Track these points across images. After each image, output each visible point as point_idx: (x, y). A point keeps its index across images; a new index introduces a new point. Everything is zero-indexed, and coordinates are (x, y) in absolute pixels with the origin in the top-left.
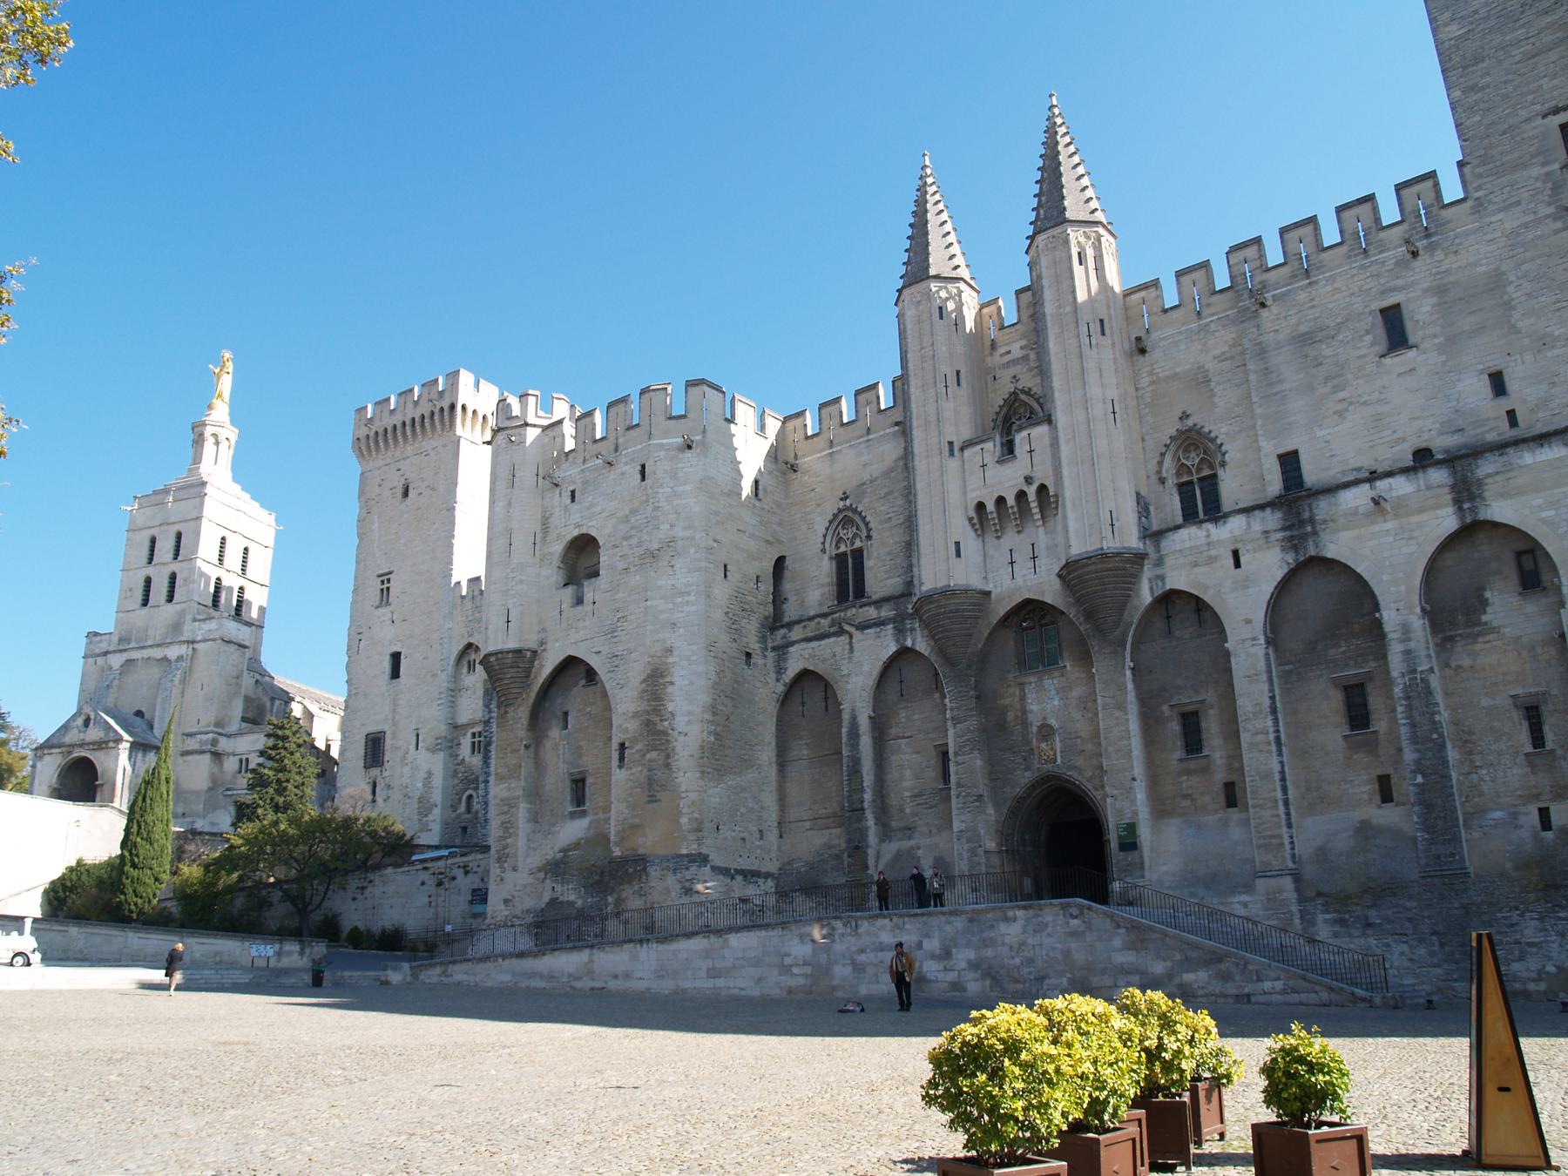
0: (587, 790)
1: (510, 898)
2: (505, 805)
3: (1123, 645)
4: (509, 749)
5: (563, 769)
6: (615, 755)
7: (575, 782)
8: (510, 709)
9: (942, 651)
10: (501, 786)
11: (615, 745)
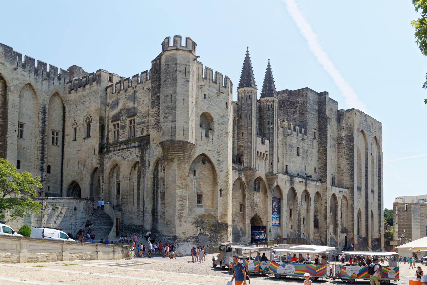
0: (203, 199)
1: (185, 232)
2: (181, 198)
3: (272, 192)
4: (182, 178)
5: (194, 190)
6: (219, 192)
7: (198, 195)
8: (183, 163)
9: (247, 182)
10: (179, 191)
11: (219, 189)
